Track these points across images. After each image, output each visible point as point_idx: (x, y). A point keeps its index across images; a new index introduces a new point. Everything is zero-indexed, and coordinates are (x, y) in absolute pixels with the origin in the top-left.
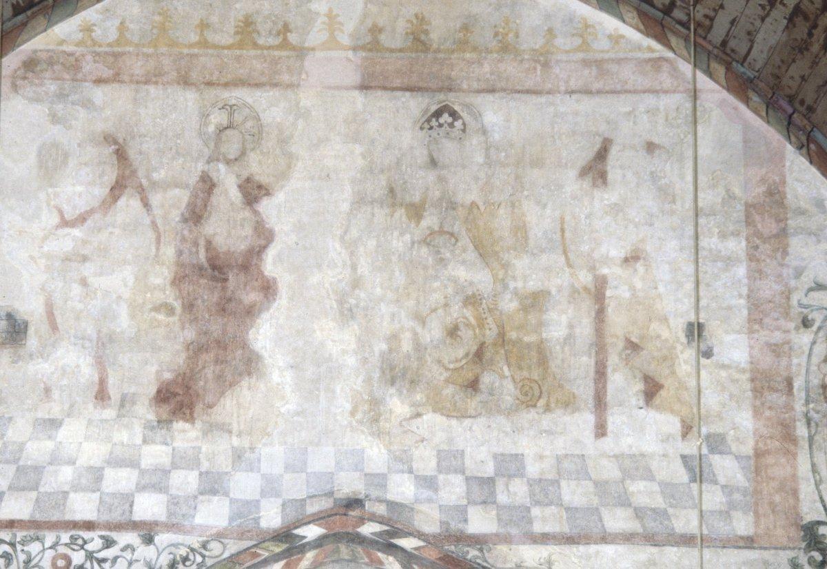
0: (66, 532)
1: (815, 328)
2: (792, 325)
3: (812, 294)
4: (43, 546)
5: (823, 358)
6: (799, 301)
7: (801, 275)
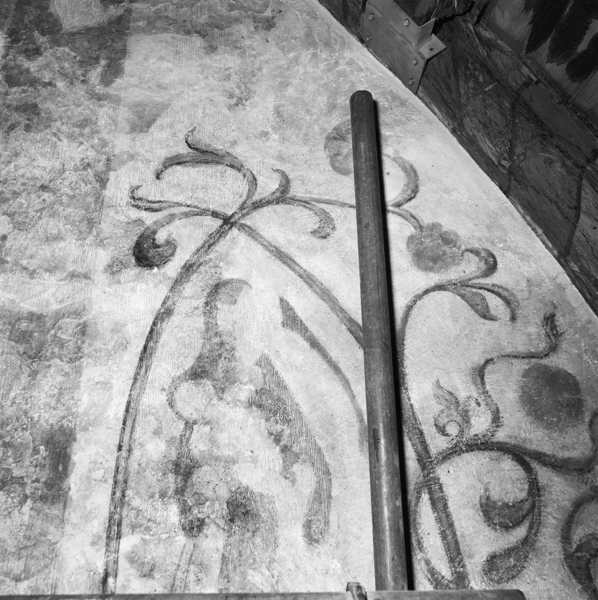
1: (173, 268)
2: (103, 257)
3: (178, 173)
5: (189, 363)
6: (134, 189)
7: (149, 125)
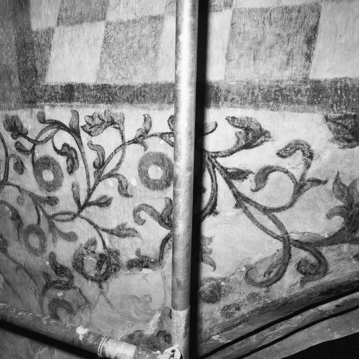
0: (160, 109)
4: (123, 137)
